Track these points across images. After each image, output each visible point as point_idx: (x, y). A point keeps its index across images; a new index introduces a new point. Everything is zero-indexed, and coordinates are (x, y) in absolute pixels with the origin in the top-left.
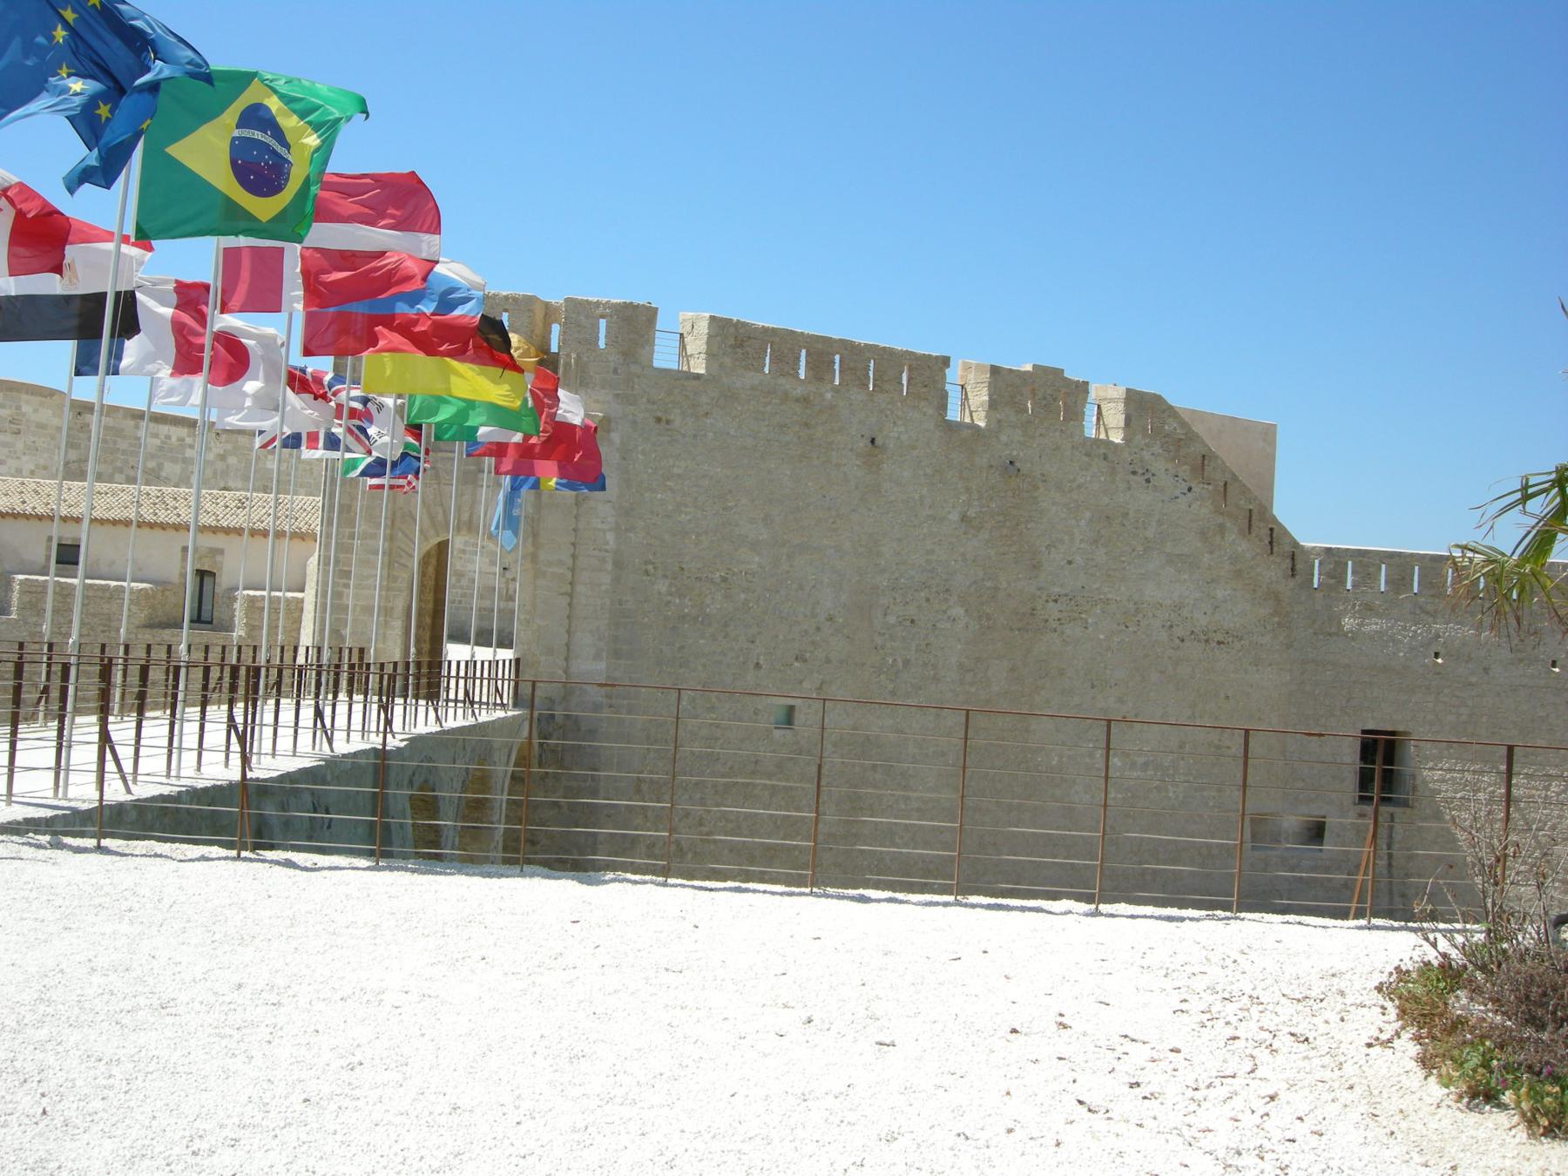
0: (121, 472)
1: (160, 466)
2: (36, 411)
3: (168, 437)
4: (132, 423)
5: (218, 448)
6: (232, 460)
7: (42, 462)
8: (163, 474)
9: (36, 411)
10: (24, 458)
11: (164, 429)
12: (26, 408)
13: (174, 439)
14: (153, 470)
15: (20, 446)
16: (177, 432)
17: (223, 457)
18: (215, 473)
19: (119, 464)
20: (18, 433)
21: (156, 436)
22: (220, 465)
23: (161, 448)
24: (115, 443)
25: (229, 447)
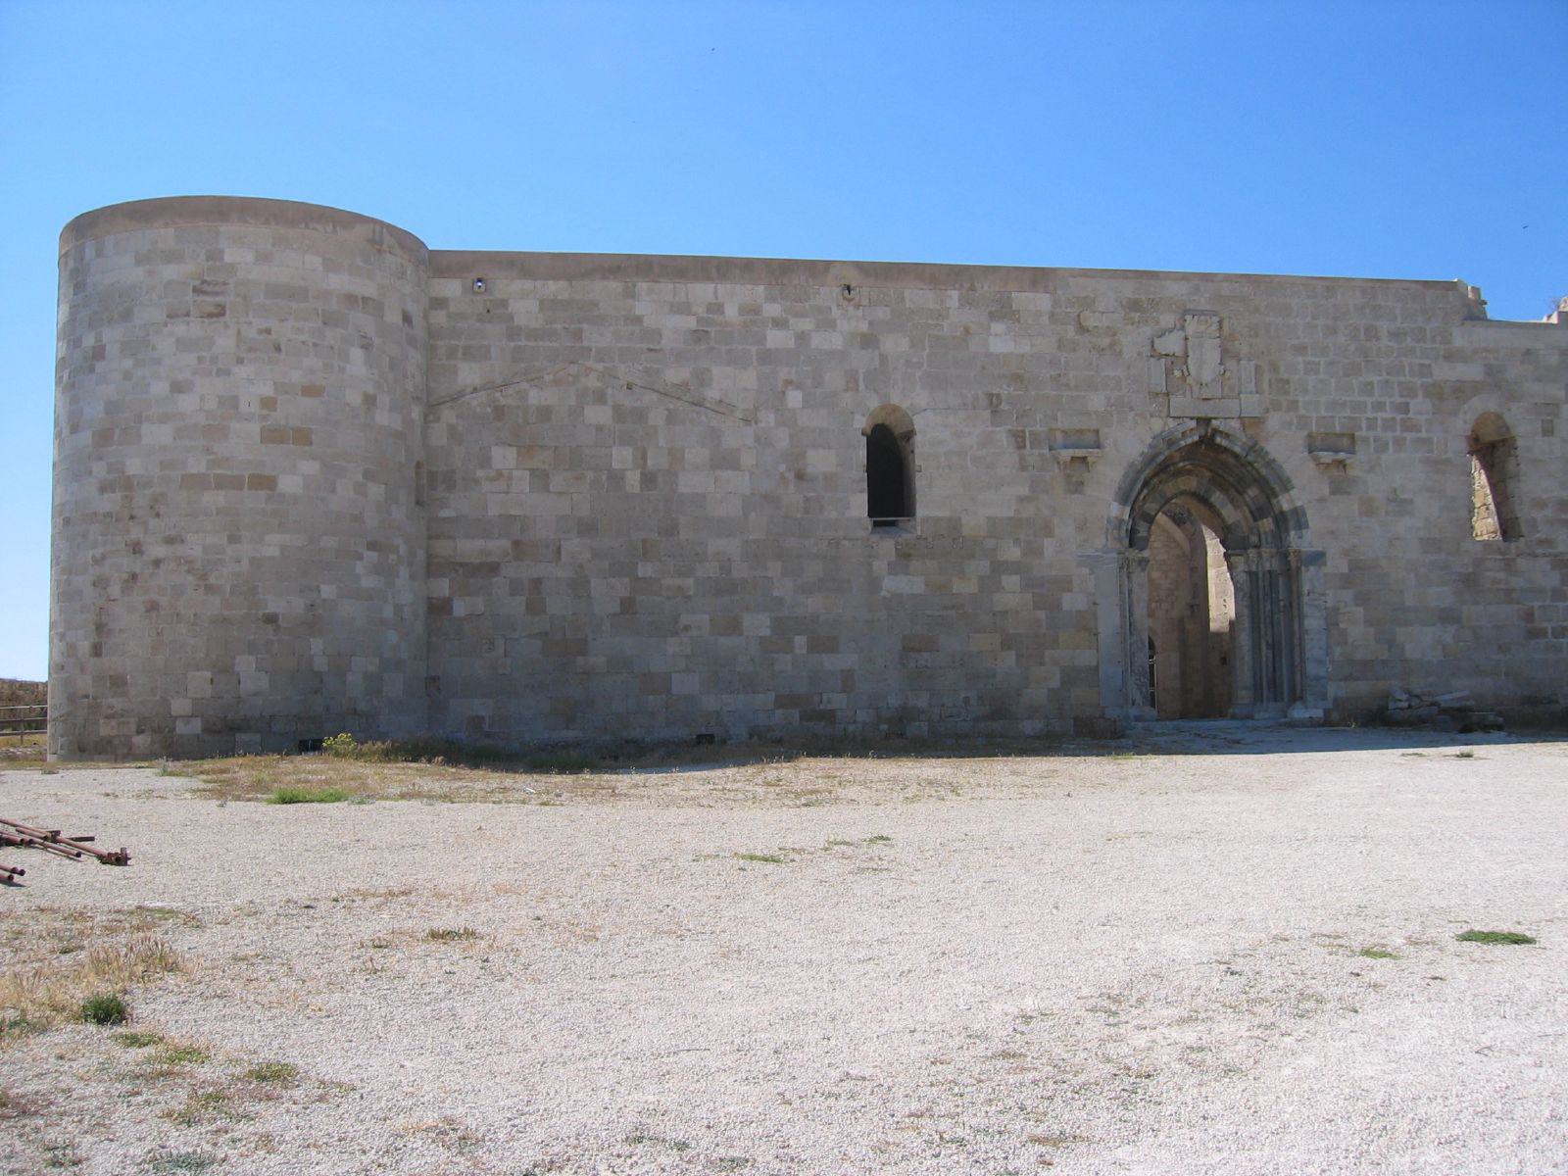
0: (600, 398)
1: (702, 378)
2: (263, 258)
3: (716, 308)
4: (614, 286)
5: (851, 322)
6: (895, 344)
7: (296, 376)
8: (712, 394)
9: (263, 258)
10: (242, 372)
11: (702, 292)
12: (230, 256)
13: (731, 312)
14: (684, 386)
15: (225, 343)
16: (734, 298)
17: (868, 341)
18: (852, 380)
19: (592, 382)
20: (220, 312)
21: (683, 309)
22: (862, 361)
23: (699, 336)
24: (578, 335)
25: (881, 313)
